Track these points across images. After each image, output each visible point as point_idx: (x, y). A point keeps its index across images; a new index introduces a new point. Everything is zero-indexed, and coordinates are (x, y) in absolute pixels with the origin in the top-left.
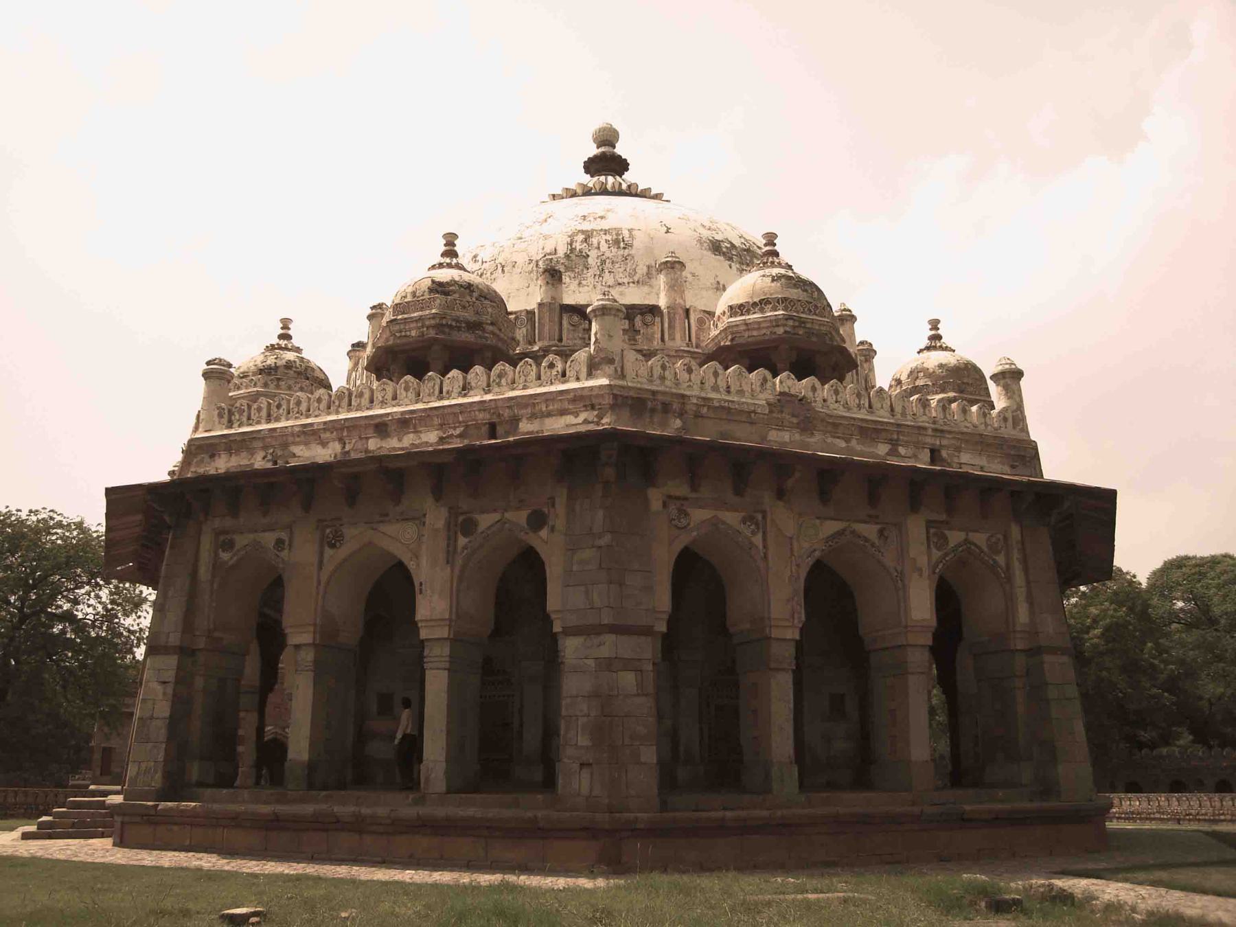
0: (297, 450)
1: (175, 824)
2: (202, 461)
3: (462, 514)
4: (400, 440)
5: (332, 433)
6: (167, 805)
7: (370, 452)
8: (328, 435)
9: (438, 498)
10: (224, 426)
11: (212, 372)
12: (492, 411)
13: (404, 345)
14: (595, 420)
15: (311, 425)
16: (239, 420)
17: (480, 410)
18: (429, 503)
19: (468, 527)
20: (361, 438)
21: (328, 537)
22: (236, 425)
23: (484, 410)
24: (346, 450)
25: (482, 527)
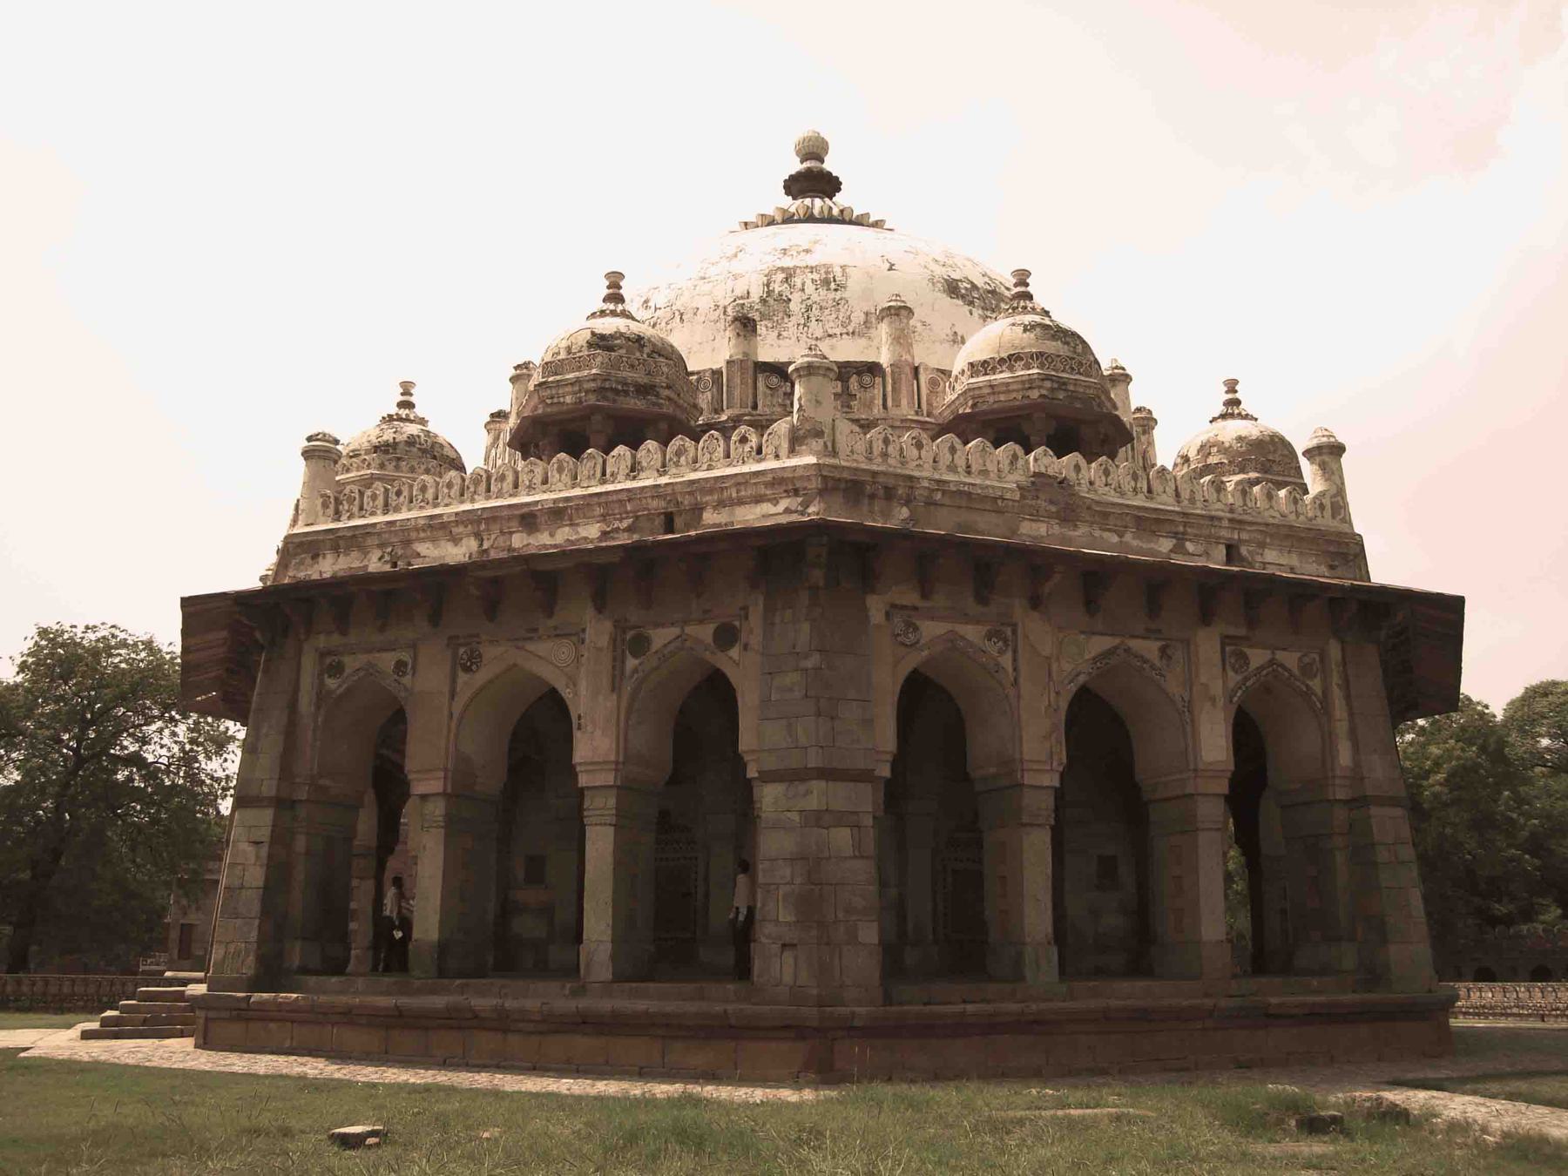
0: (422, 548)
1: (272, 1020)
2: (302, 563)
4: (552, 535)
5: (466, 527)
6: (261, 996)
7: (514, 550)
8: (461, 529)
9: (600, 609)
11: (314, 450)
12: (668, 498)
13: (561, 413)
14: (800, 508)
15: (441, 516)
16: (348, 511)
17: (653, 497)
18: (589, 613)
19: (640, 645)
21: (462, 659)
22: (344, 517)
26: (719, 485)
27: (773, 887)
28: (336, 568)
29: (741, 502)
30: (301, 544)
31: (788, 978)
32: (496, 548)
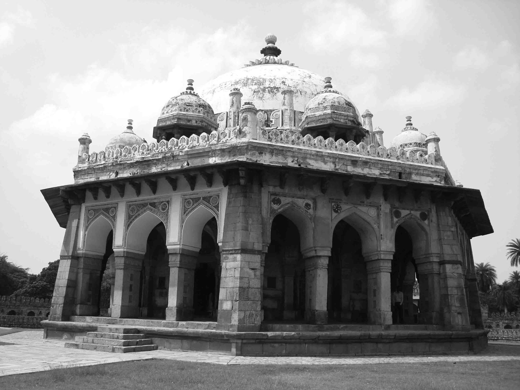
1: (275, 343)
2: (253, 154)
3: (395, 208)
4: (363, 170)
5: (330, 159)
7: (348, 171)
8: (328, 159)
9: (386, 199)
10: (266, 140)
11: (253, 109)
13: (338, 125)
14: (439, 181)
15: (322, 152)
16: (275, 139)
18: (382, 201)
19: (397, 214)
20: (343, 164)
21: (333, 207)
23: (400, 167)
24: (337, 168)
25: (402, 215)
26: (419, 168)
27: (453, 295)
28: (271, 160)
29: (423, 175)
30: (255, 147)
31: (460, 323)
32: (341, 169)
